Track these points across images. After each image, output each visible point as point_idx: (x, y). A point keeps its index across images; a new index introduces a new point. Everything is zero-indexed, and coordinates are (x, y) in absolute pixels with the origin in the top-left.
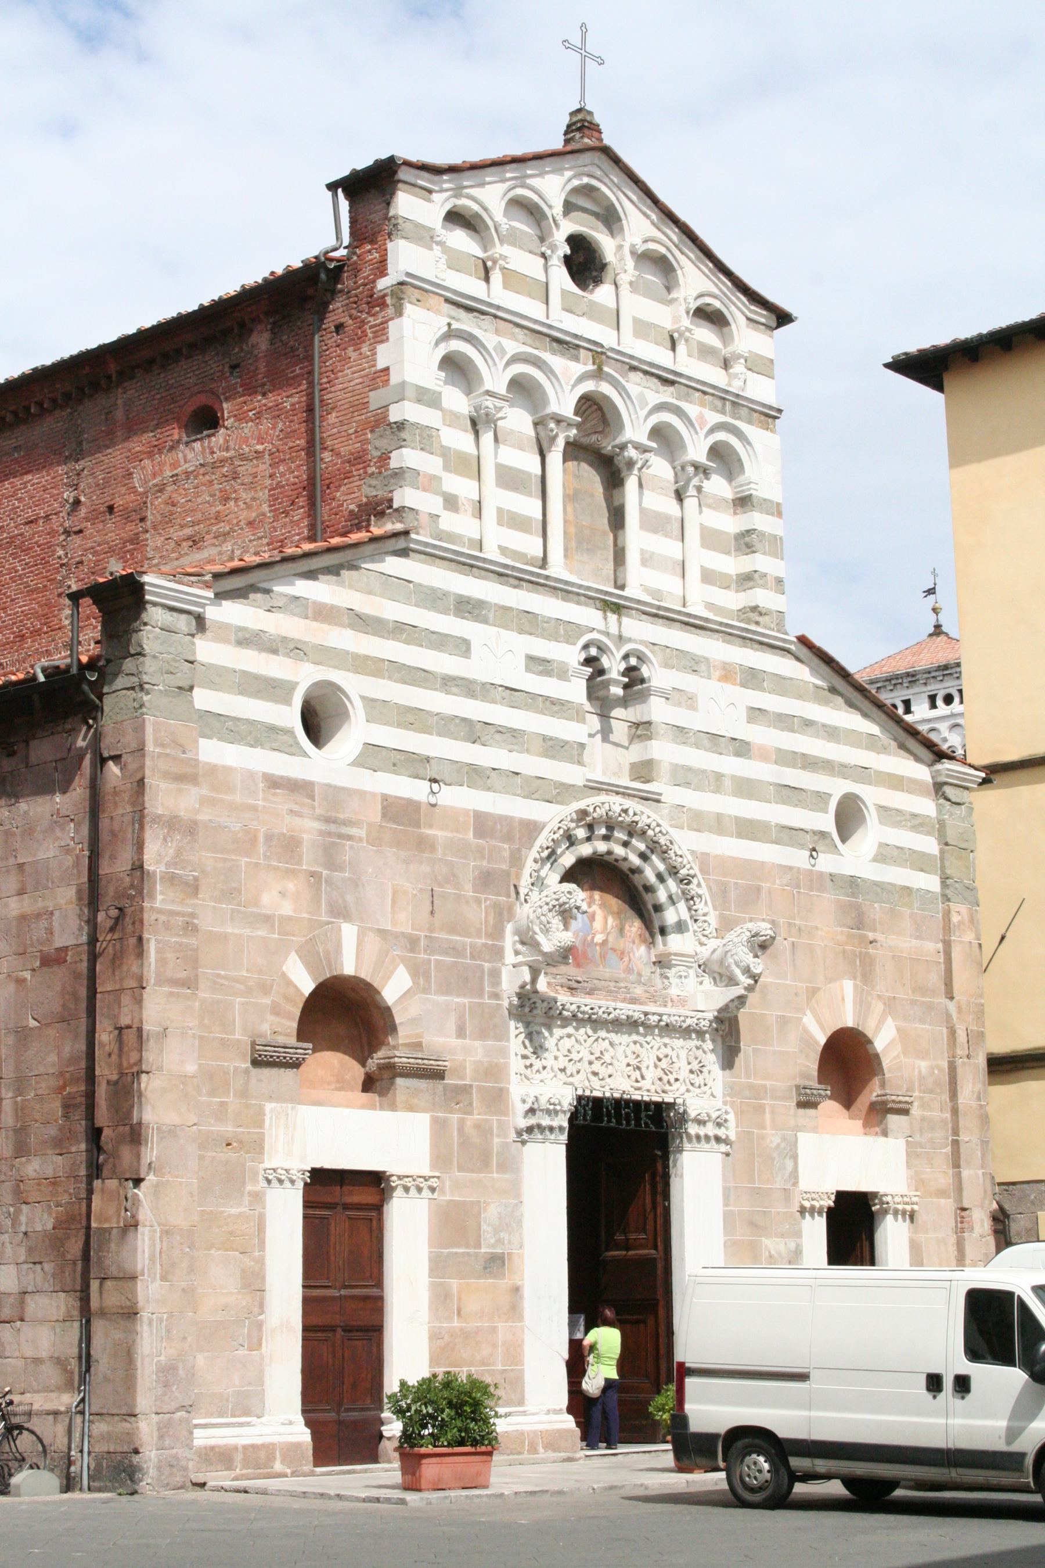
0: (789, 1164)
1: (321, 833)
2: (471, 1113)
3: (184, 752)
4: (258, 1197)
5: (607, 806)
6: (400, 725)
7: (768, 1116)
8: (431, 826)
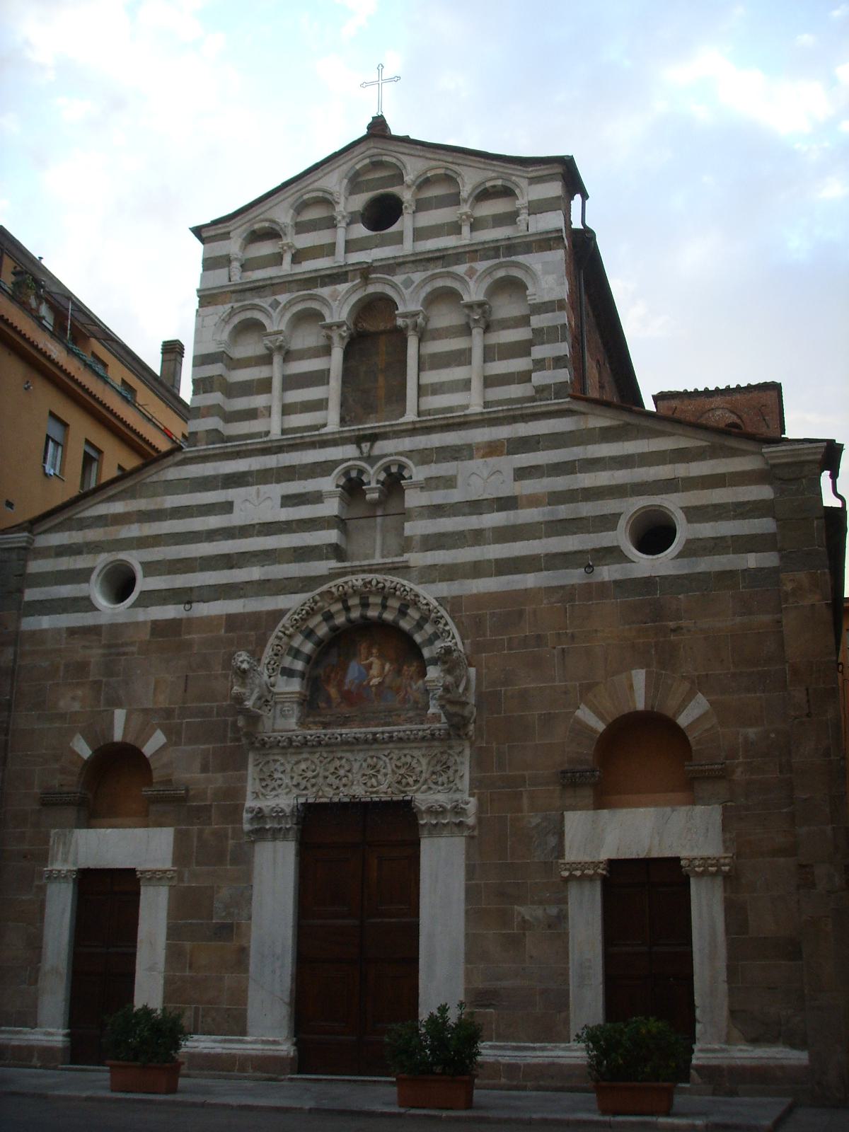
0: (552, 841)
1: (104, 655)
2: (210, 824)
3: (6, 628)
4: (42, 889)
5: (350, 583)
6: (169, 573)
7: (525, 801)
8: (189, 633)
